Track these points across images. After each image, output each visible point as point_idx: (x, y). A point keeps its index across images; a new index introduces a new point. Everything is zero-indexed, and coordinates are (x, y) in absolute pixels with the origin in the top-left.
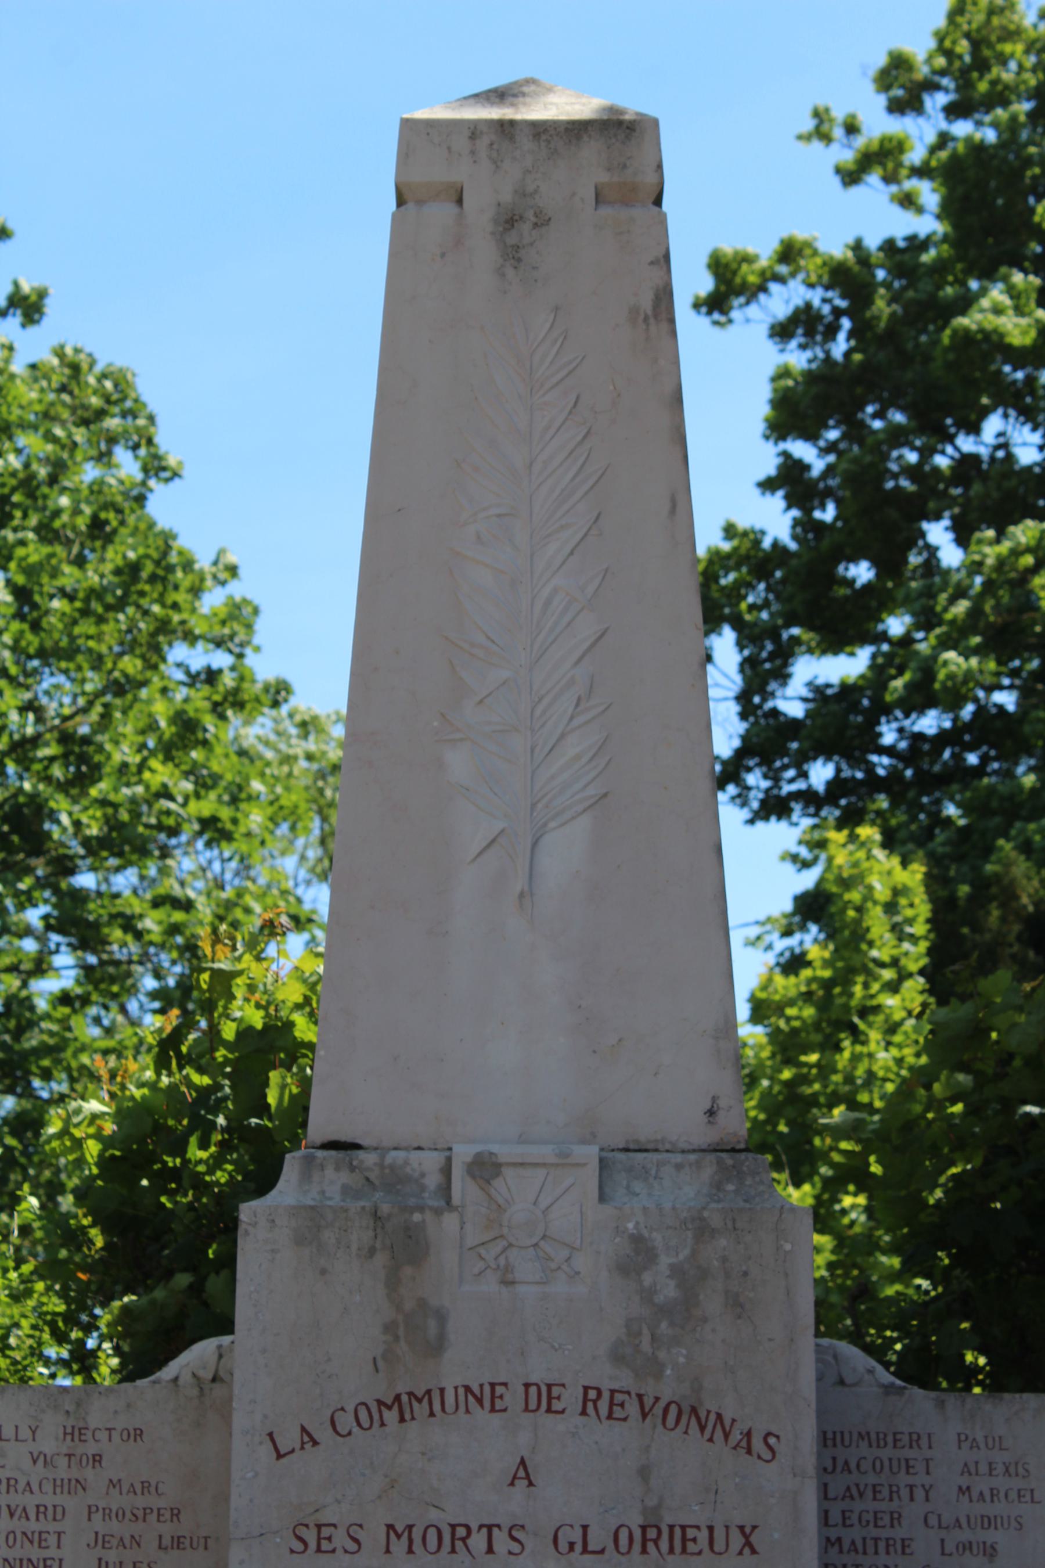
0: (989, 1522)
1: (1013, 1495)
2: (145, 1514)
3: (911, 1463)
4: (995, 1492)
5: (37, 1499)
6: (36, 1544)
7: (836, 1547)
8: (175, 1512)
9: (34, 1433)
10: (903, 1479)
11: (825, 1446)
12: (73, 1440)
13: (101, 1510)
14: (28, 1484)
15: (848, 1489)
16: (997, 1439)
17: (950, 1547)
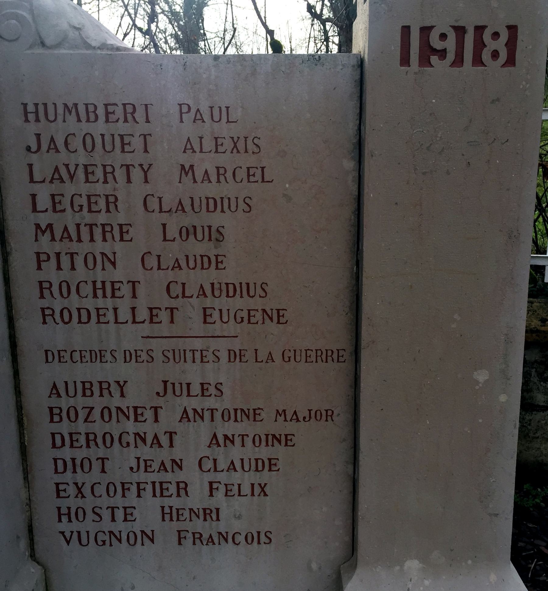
1: (242, 174)
3: (127, 140)
4: (222, 171)
7: (48, 234)
11: (27, 120)
15: (57, 169)
16: (224, 110)
17: (173, 231)
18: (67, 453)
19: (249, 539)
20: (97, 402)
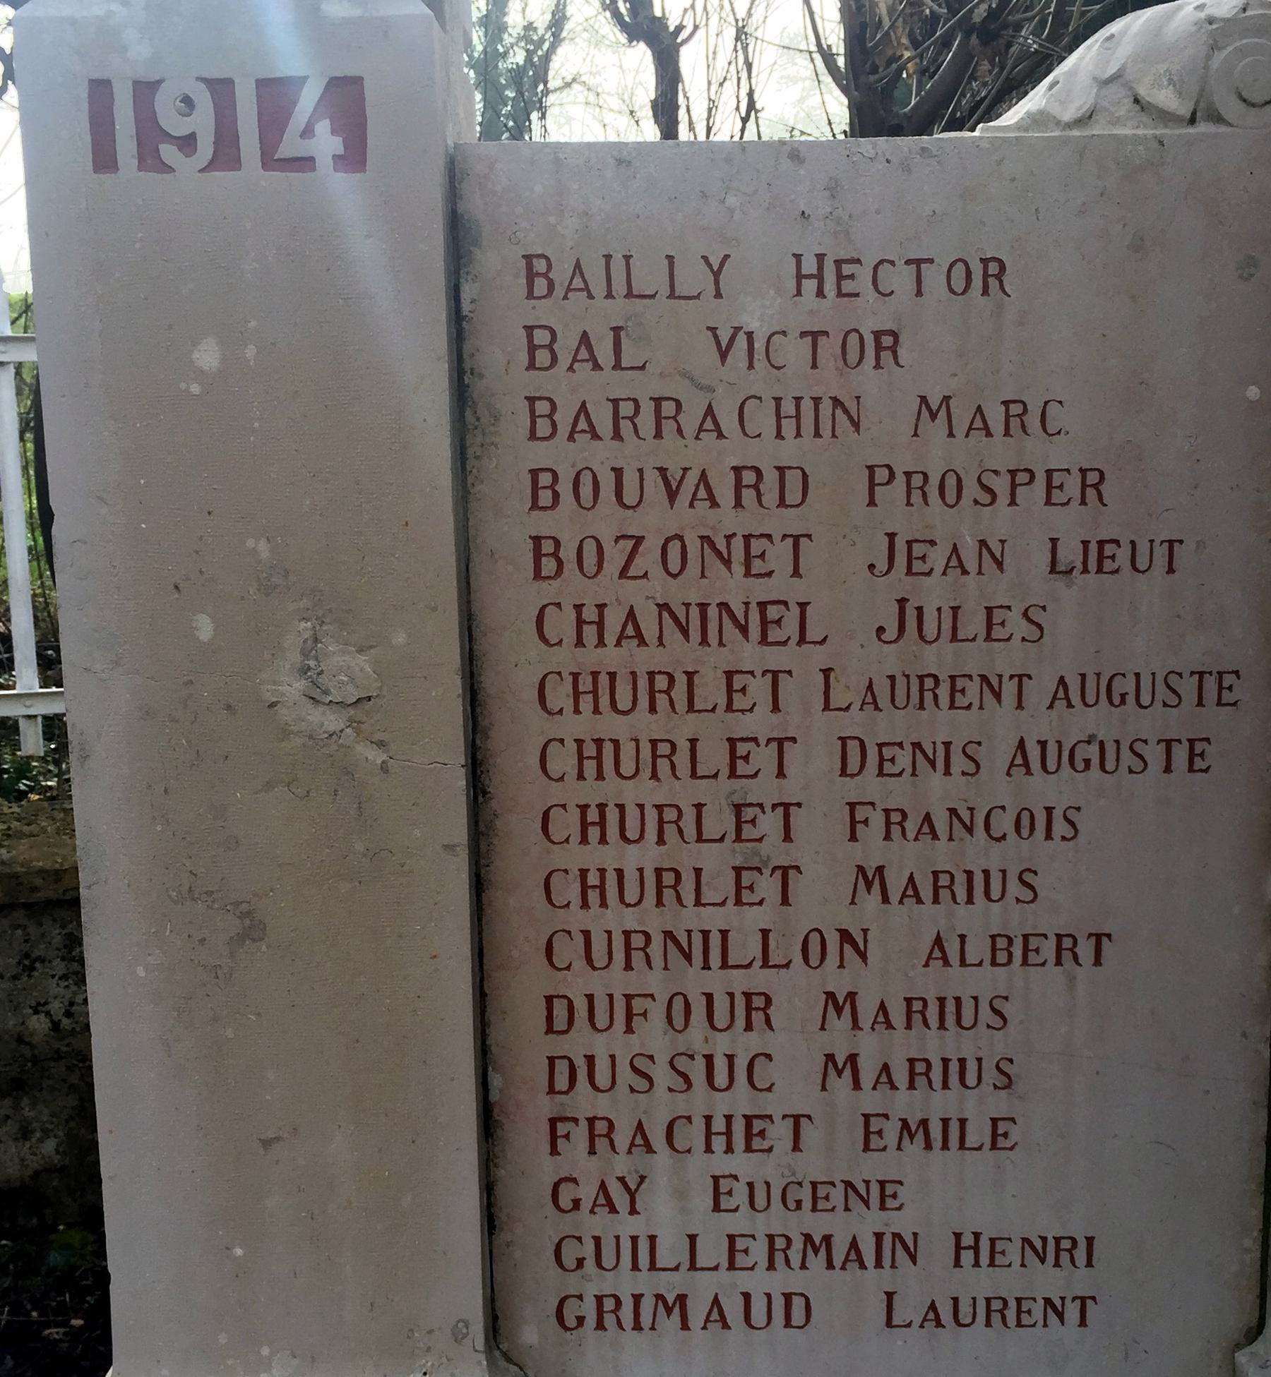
2: (1014, 486)
5: (735, 451)
6: (738, 569)
8: (1092, 478)
9: (717, 275)
12: (820, 293)
13: (900, 479)
14: (710, 411)
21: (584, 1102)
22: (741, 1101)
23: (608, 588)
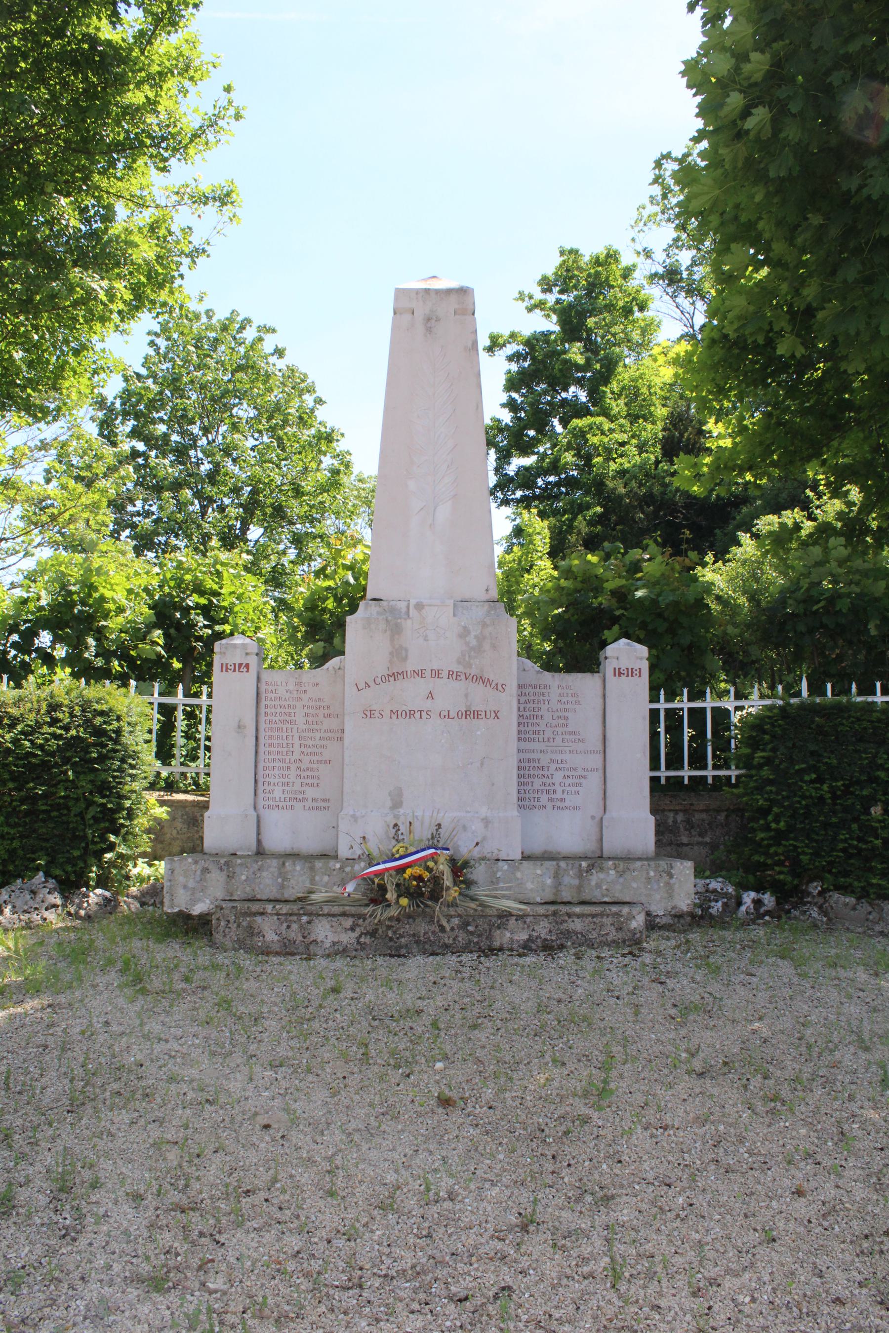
0: (566, 710)
10: (542, 698)
18: (522, 780)
19: (575, 808)
20: (532, 765)
21: (267, 779)
22: (286, 780)
23: (274, 718)
